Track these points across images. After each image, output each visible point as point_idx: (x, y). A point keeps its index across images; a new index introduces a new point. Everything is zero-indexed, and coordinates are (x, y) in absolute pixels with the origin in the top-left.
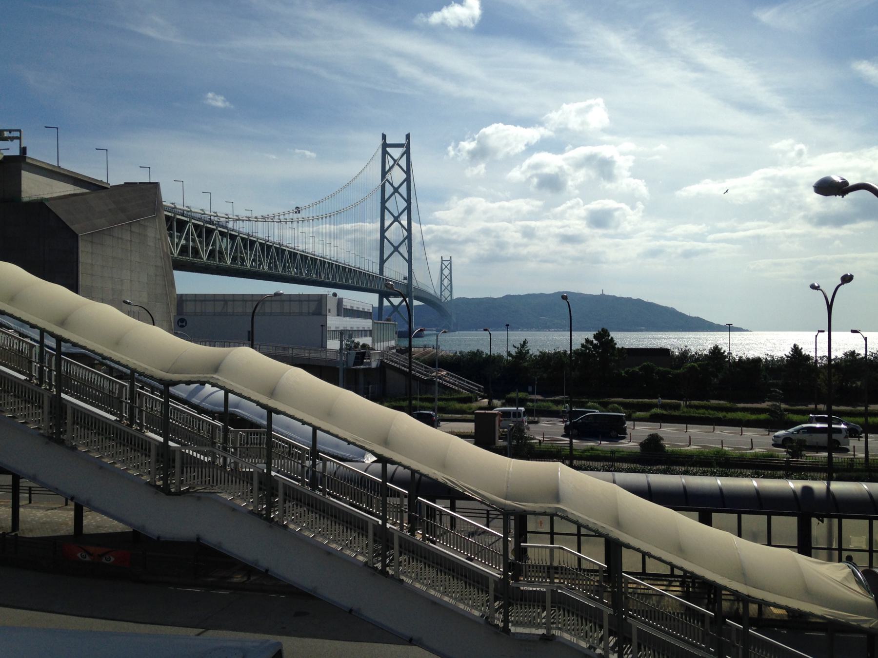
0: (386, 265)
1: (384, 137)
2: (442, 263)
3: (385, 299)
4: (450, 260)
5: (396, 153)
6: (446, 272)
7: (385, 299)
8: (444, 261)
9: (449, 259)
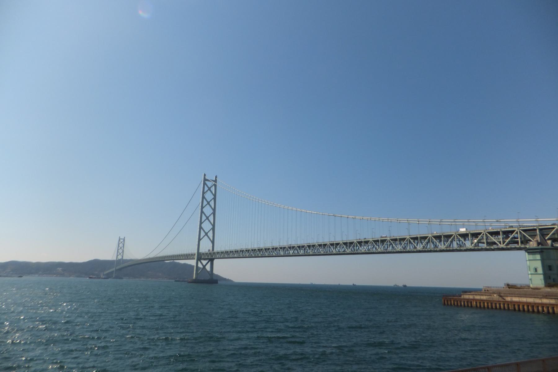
0: (201, 241)
1: (205, 175)
2: (119, 240)
3: (199, 262)
4: (124, 239)
5: (209, 184)
6: (121, 245)
7: (199, 262)
8: (121, 239)
9: (123, 238)
